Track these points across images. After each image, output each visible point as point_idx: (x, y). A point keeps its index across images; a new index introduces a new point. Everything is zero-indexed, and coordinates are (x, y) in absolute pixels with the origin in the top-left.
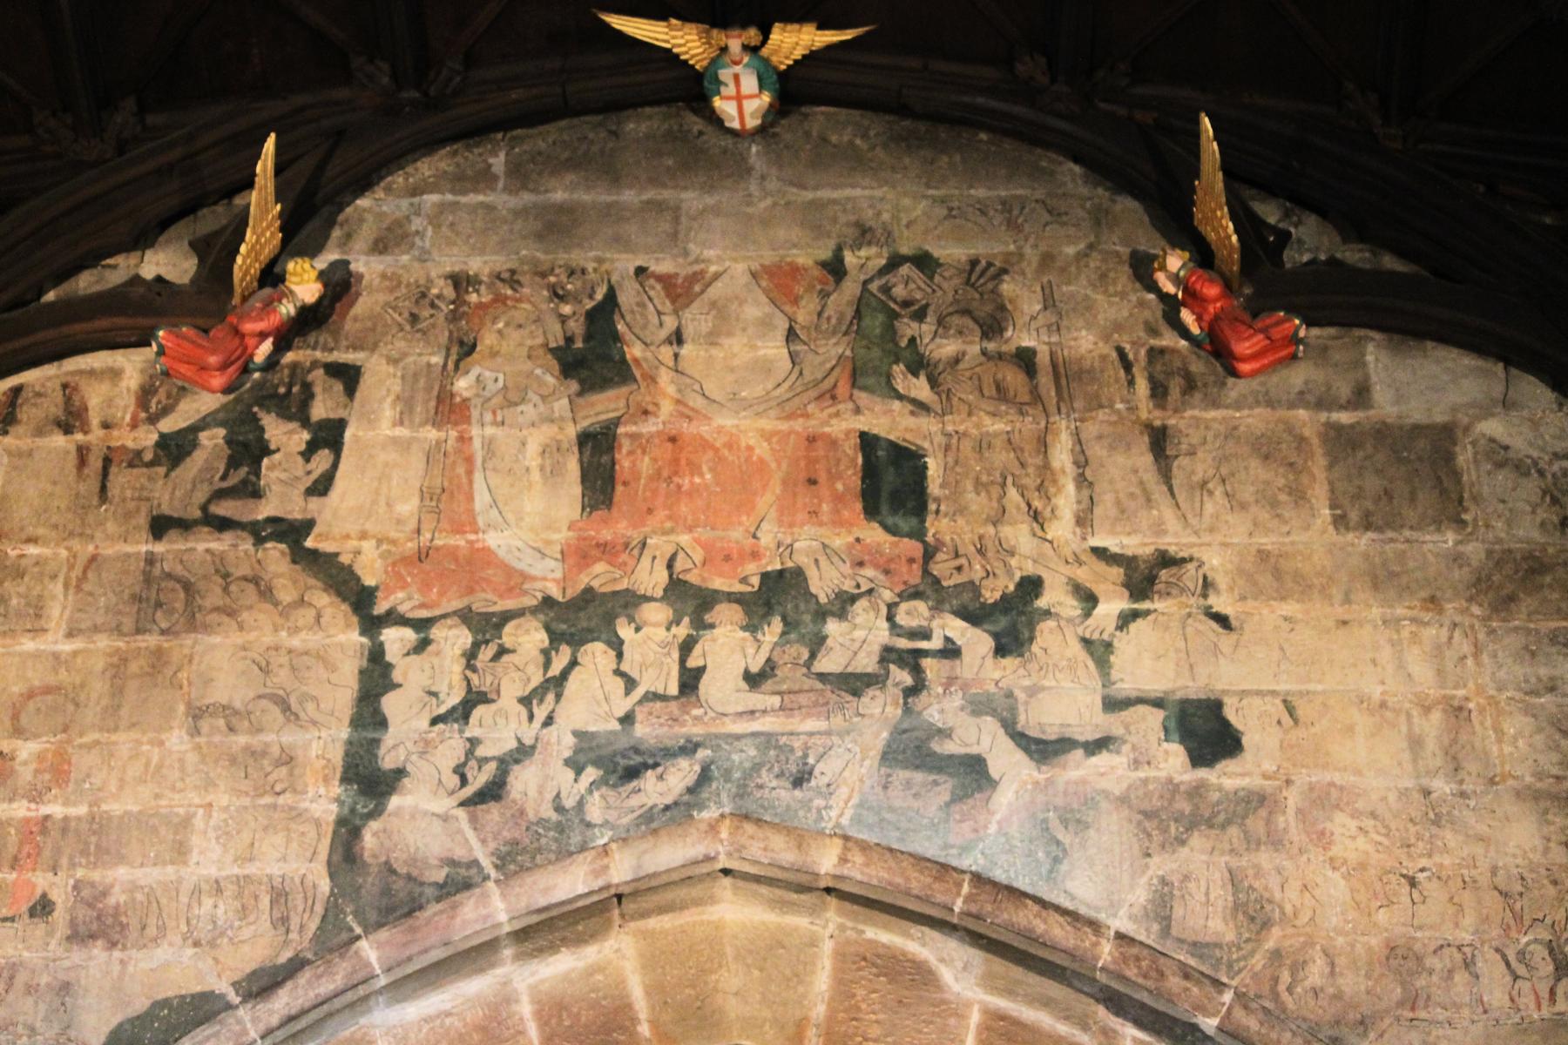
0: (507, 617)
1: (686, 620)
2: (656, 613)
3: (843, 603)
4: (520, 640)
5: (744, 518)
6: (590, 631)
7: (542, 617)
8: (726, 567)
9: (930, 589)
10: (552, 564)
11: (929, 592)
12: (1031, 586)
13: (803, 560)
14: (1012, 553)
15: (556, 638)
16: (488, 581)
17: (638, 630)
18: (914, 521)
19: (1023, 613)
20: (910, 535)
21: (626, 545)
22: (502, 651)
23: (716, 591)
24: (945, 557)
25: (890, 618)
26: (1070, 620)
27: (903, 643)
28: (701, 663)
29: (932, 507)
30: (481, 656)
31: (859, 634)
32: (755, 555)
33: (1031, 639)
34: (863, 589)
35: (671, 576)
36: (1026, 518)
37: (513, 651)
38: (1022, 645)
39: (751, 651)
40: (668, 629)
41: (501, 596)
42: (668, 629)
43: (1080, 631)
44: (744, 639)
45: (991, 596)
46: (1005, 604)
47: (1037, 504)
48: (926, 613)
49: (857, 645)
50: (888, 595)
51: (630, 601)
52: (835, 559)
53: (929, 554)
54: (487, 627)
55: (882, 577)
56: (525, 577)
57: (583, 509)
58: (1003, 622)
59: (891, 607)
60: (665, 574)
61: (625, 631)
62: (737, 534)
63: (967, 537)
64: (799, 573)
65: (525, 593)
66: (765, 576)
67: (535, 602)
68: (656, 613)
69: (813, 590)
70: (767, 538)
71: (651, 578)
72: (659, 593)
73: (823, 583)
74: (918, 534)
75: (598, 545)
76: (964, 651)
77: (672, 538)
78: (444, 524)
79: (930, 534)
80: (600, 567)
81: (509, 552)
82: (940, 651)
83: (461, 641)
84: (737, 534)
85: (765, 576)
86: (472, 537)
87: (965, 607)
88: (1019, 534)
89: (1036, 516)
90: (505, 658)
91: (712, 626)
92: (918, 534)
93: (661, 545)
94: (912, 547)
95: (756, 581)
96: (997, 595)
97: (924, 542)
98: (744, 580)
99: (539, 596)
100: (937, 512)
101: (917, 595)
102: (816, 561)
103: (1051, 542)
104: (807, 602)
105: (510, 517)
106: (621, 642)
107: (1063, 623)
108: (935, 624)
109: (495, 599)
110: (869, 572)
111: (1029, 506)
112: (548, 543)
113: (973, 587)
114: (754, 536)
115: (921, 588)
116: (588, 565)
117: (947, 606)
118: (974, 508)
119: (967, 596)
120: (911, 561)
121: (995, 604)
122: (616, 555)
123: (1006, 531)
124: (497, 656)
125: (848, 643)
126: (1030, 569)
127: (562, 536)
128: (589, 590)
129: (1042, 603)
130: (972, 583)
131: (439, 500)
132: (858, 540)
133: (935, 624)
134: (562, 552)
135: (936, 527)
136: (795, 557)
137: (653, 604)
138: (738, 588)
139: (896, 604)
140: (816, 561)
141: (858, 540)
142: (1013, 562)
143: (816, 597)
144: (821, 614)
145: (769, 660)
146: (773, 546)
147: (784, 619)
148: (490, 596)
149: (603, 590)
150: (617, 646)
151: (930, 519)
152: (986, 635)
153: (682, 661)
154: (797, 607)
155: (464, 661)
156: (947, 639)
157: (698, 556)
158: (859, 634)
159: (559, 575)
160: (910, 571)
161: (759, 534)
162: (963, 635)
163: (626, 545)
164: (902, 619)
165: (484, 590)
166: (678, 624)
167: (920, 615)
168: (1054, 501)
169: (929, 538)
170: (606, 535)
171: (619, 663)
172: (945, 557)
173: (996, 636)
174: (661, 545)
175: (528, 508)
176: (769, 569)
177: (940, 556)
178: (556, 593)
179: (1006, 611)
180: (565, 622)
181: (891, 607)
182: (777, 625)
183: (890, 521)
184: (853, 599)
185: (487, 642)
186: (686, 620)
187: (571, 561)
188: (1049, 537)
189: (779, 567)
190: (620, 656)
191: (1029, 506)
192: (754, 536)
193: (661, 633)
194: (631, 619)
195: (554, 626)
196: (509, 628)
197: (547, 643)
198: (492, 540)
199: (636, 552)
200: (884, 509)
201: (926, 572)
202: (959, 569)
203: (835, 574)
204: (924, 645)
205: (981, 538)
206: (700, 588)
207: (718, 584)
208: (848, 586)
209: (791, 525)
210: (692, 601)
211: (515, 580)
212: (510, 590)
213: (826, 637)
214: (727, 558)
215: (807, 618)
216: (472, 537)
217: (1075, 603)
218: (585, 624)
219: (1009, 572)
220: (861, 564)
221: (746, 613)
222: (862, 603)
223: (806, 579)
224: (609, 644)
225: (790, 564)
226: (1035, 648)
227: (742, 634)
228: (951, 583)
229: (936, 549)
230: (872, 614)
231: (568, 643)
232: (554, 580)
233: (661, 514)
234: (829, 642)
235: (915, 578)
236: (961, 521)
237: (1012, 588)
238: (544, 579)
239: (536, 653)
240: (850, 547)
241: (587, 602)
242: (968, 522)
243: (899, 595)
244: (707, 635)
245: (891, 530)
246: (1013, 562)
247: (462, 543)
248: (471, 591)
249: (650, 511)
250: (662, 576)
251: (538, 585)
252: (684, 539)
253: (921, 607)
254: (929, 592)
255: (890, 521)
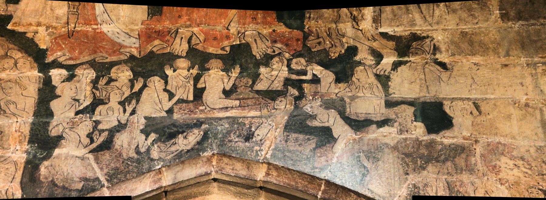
0: (113, 64)
1: (197, 66)
2: (183, 63)
3: (267, 60)
4: (119, 75)
5: (223, 21)
6: (152, 71)
7: (129, 64)
8: (215, 43)
10: (134, 40)
11: (306, 54)
12: (353, 51)
13: (249, 40)
14: (343, 36)
15: (136, 75)
16: (104, 48)
17: (174, 71)
18: (299, 22)
19: (348, 63)
20: (297, 29)
21: (169, 32)
22: (111, 80)
23: (210, 54)
24: (313, 38)
25: (288, 66)
26: (370, 66)
27: (294, 77)
28: (203, 86)
30: (100, 83)
31: (275, 73)
32: (228, 37)
33: (352, 75)
35: (189, 46)
36: (350, 19)
37: (116, 80)
38: (348, 77)
39: (226, 81)
40: (188, 71)
41: (110, 55)
42: (188, 71)
43: (374, 71)
44: (222, 75)
45: (334, 55)
46: (340, 58)
48: (305, 64)
49: (274, 78)
50: (287, 55)
51: (170, 59)
52: (264, 39)
53: (306, 37)
54: (103, 69)
56: (121, 46)
57: (148, 15)
58: (339, 67)
59: (289, 61)
60: (187, 45)
61: (169, 72)
62: (219, 28)
63: (323, 29)
64: (247, 46)
65: (121, 53)
66: (232, 47)
67: (126, 58)
68: (183, 63)
69: (254, 53)
70: (233, 30)
71: (180, 47)
72: (184, 54)
73: (258, 50)
75: (155, 32)
76: (321, 80)
77: (190, 29)
78: (81, 20)
79: (307, 27)
80: (157, 42)
81: (113, 34)
82: (311, 80)
83: (90, 76)
84: (219, 28)
85: (232, 47)
86: (95, 27)
90: (112, 84)
91: (209, 69)
93: (184, 32)
95: (228, 49)
96: (337, 55)
97: (304, 32)
98: (223, 49)
99: (128, 55)
100: (310, 17)
101: (300, 55)
102: (255, 40)
103: (361, 31)
104: (251, 58)
105: (113, 18)
106: (167, 76)
108: (308, 68)
109: (107, 56)
110: (279, 45)
111: (351, 14)
112: (132, 30)
113: (326, 52)
114: (227, 29)
115: (302, 52)
116: (151, 41)
117: (314, 60)
119: (323, 56)
120: (298, 40)
122: (165, 36)
123: (341, 26)
124: (108, 83)
125: (269, 77)
126: (352, 42)
127: (139, 27)
128: (152, 52)
129: (357, 58)
130: (325, 49)
131: (78, 9)
132: (274, 31)
133: (308, 68)
134: (139, 35)
136: (245, 39)
137: (182, 59)
138: (220, 52)
139: (291, 59)
140: (255, 40)
141: (274, 31)
142: (344, 40)
143: (255, 56)
144: (258, 64)
145: (234, 84)
146: (235, 33)
147: (241, 66)
148: (104, 55)
149: (158, 52)
150: (165, 78)
151: (306, 21)
153: (195, 85)
154: (246, 61)
155: (92, 85)
156: (314, 75)
157: (202, 38)
158: (275, 73)
159: (137, 45)
160: (297, 45)
161: (230, 28)
162: (321, 73)
163: (169, 32)
164: (294, 66)
165: (101, 52)
166: (193, 69)
167: (302, 64)
169: (306, 30)
170: (159, 27)
171: (166, 86)
172: (313, 38)
173: (336, 73)
174: (184, 32)
175: (122, 14)
176: (234, 43)
177: (311, 38)
178: (135, 53)
180: (141, 67)
181: (289, 61)
182: (238, 69)
183: (288, 22)
184: (272, 57)
185: (103, 76)
186: (197, 66)
187: (143, 39)
188: (360, 28)
189: (238, 43)
190: (166, 83)
191: (351, 14)
192: (227, 29)
193: (185, 73)
194: (171, 66)
195: (135, 69)
196: (114, 70)
197: (132, 76)
198: (105, 28)
199: (173, 35)
201: (305, 45)
202: (319, 43)
203: (263, 46)
204: (304, 78)
206: (202, 52)
207: (211, 50)
208: (269, 51)
209: (244, 24)
210: (199, 59)
211: (117, 47)
212: (114, 52)
213: (260, 74)
214: (215, 39)
215: (251, 66)
216: (95, 27)
217: (372, 58)
218: (150, 68)
219: (342, 44)
220: (275, 42)
221: (224, 64)
222: (276, 59)
223: (251, 49)
224: (161, 77)
225: (244, 42)
226: (354, 79)
227: (222, 73)
228: (315, 50)
229: (309, 35)
230: (280, 64)
231: (142, 77)
232: (135, 48)
233: (185, 18)
234: (261, 76)
235: (299, 48)
237: (343, 51)
238: (131, 47)
239: (126, 81)
240: (271, 34)
241: (151, 58)
242: (323, 22)
244: (207, 73)
246: (344, 40)
247: (90, 29)
248: (95, 52)
249: (180, 17)
250: (185, 46)
251: (128, 50)
252: (196, 30)
253: (302, 60)
254: (306, 54)
255: (288, 22)
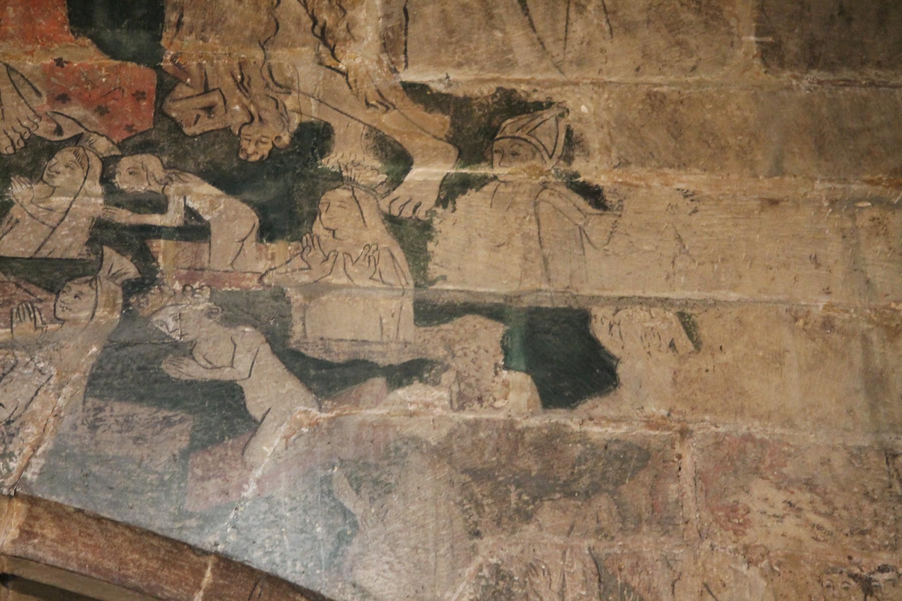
9: (167, 139)
11: (164, 143)
12: (315, 138)
18: (143, 37)
19: (301, 176)
20: (137, 58)
24: (190, 92)
25: (106, 179)
26: (371, 189)
27: (124, 217)
29: (172, 17)
31: (60, 201)
33: (314, 215)
34: (66, 136)
36: (310, 37)
38: (300, 223)
43: (384, 204)
45: (255, 150)
47: (325, 17)
48: (160, 174)
49: (56, 216)
50: (102, 145)
52: (26, 90)
53: (165, 87)
55: (94, 118)
59: (108, 163)
63: (222, 63)
74: (150, 57)
76: (214, 229)
82: (178, 229)
87: (217, 167)
88: (299, 62)
89: (324, 35)
92: (150, 57)
94: (137, 74)
96: (265, 149)
97: (158, 69)
100: (179, 24)
101: (146, 146)
103: (345, 74)
107: (359, 193)
108: (171, 190)
110: (76, 111)
113: (229, 137)
115: (153, 136)
117: (191, 164)
118: (233, 20)
119: (220, 150)
120: (139, 96)
121: (261, 161)
123: (281, 56)
125: (42, 214)
126: (314, 112)
129: (330, 162)
130: (227, 130)
132: (59, 62)
133: (171, 190)
135: (179, 46)
139: (116, 159)
141: (59, 62)
152: (245, 207)
156: (190, 212)
158: (60, 201)
162: (213, 206)
164: (123, 181)
167: (150, 176)
168: (350, 13)
172: (190, 92)
173: (261, 209)
177: (182, 91)
179: (276, 174)
181: (108, 163)
183: (107, 35)
184: (52, 149)
188: (342, 67)
200: (100, 15)
201: (161, 113)
202: (209, 109)
203: (24, 111)
204: (155, 219)
205: (241, 66)
208: (44, 129)
213: (11, 204)
217: (378, 164)
219: (283, 115)
220: (64, 98)
222: (66, 156)
229: (177, 81)
230: (79, 172)
234: (15, 212)
235: (144, 122)
236: (213, 39)
237: (286, 139)
240: (48, 72)
242: (223, 42)
243: (120, 146)
245: (110, 50)
246: (290, 102)
253: (152, 163)
254: (164, 143)
255: (107, 35)
